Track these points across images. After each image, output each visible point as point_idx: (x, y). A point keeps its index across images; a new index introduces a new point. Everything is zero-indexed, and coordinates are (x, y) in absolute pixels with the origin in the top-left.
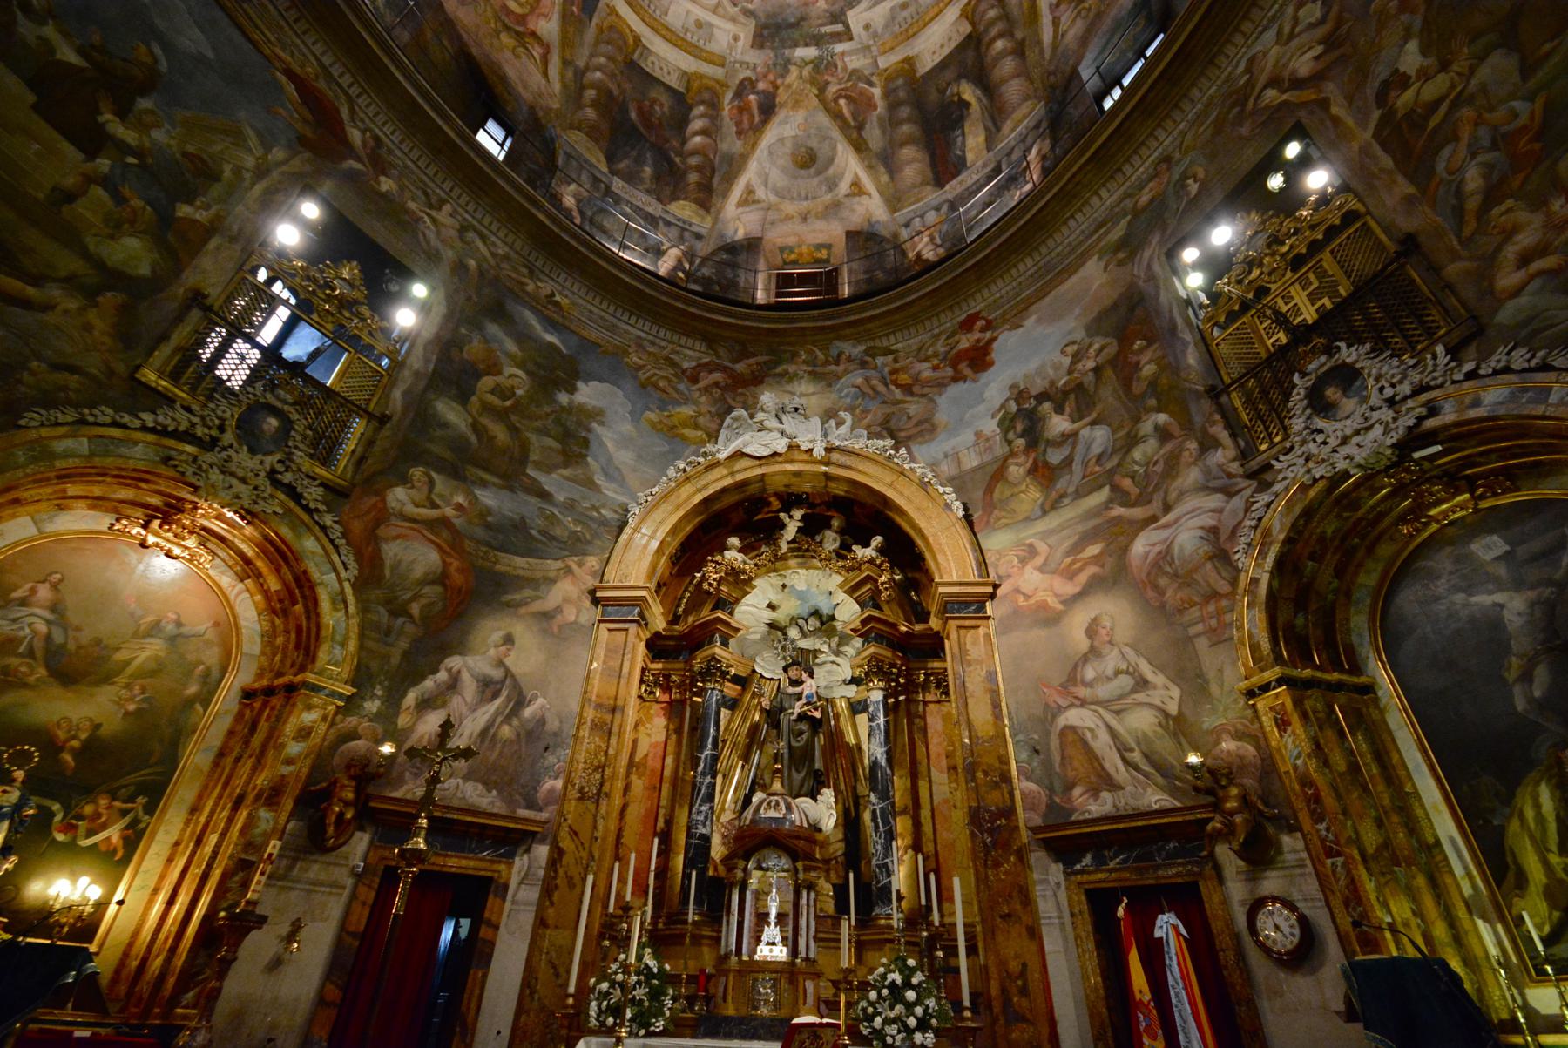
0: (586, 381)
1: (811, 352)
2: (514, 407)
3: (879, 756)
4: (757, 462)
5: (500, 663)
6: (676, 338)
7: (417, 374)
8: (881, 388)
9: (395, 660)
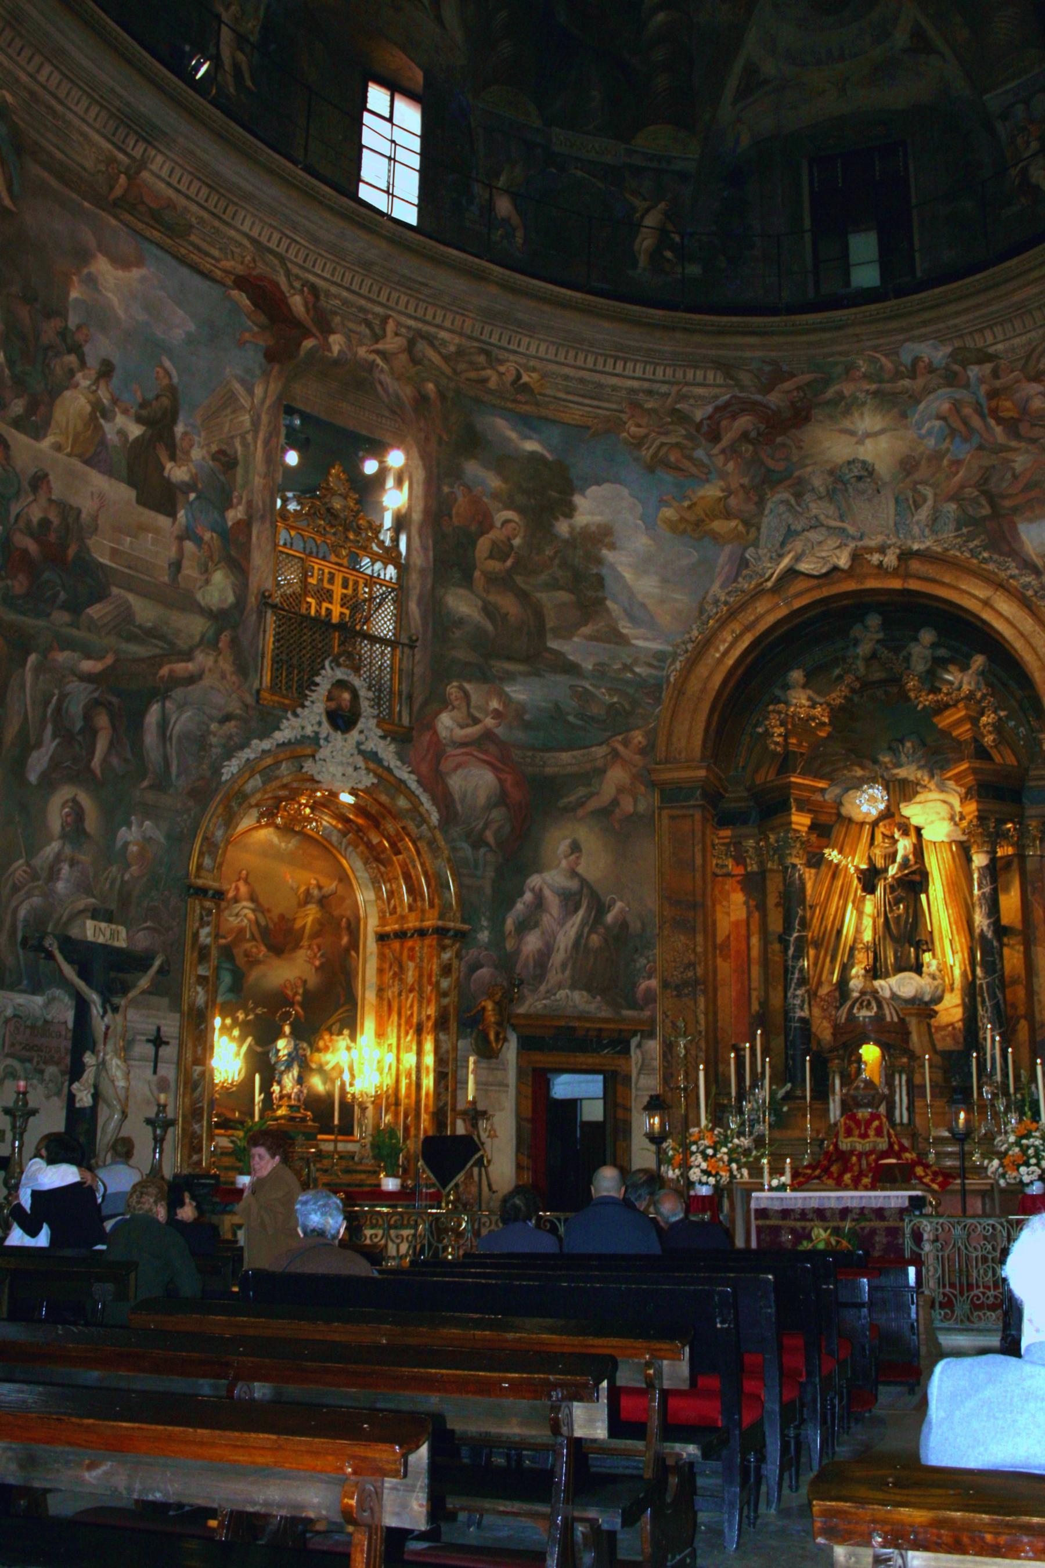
0: (582, 492)
1: (873, 360)
2: (516, 564)
3: (985, 928)
4: (815, 582)
5: (573, 874)
6: (679, 374)
7: (422, 572)
8: (976, 422)
9: (488, 890)
